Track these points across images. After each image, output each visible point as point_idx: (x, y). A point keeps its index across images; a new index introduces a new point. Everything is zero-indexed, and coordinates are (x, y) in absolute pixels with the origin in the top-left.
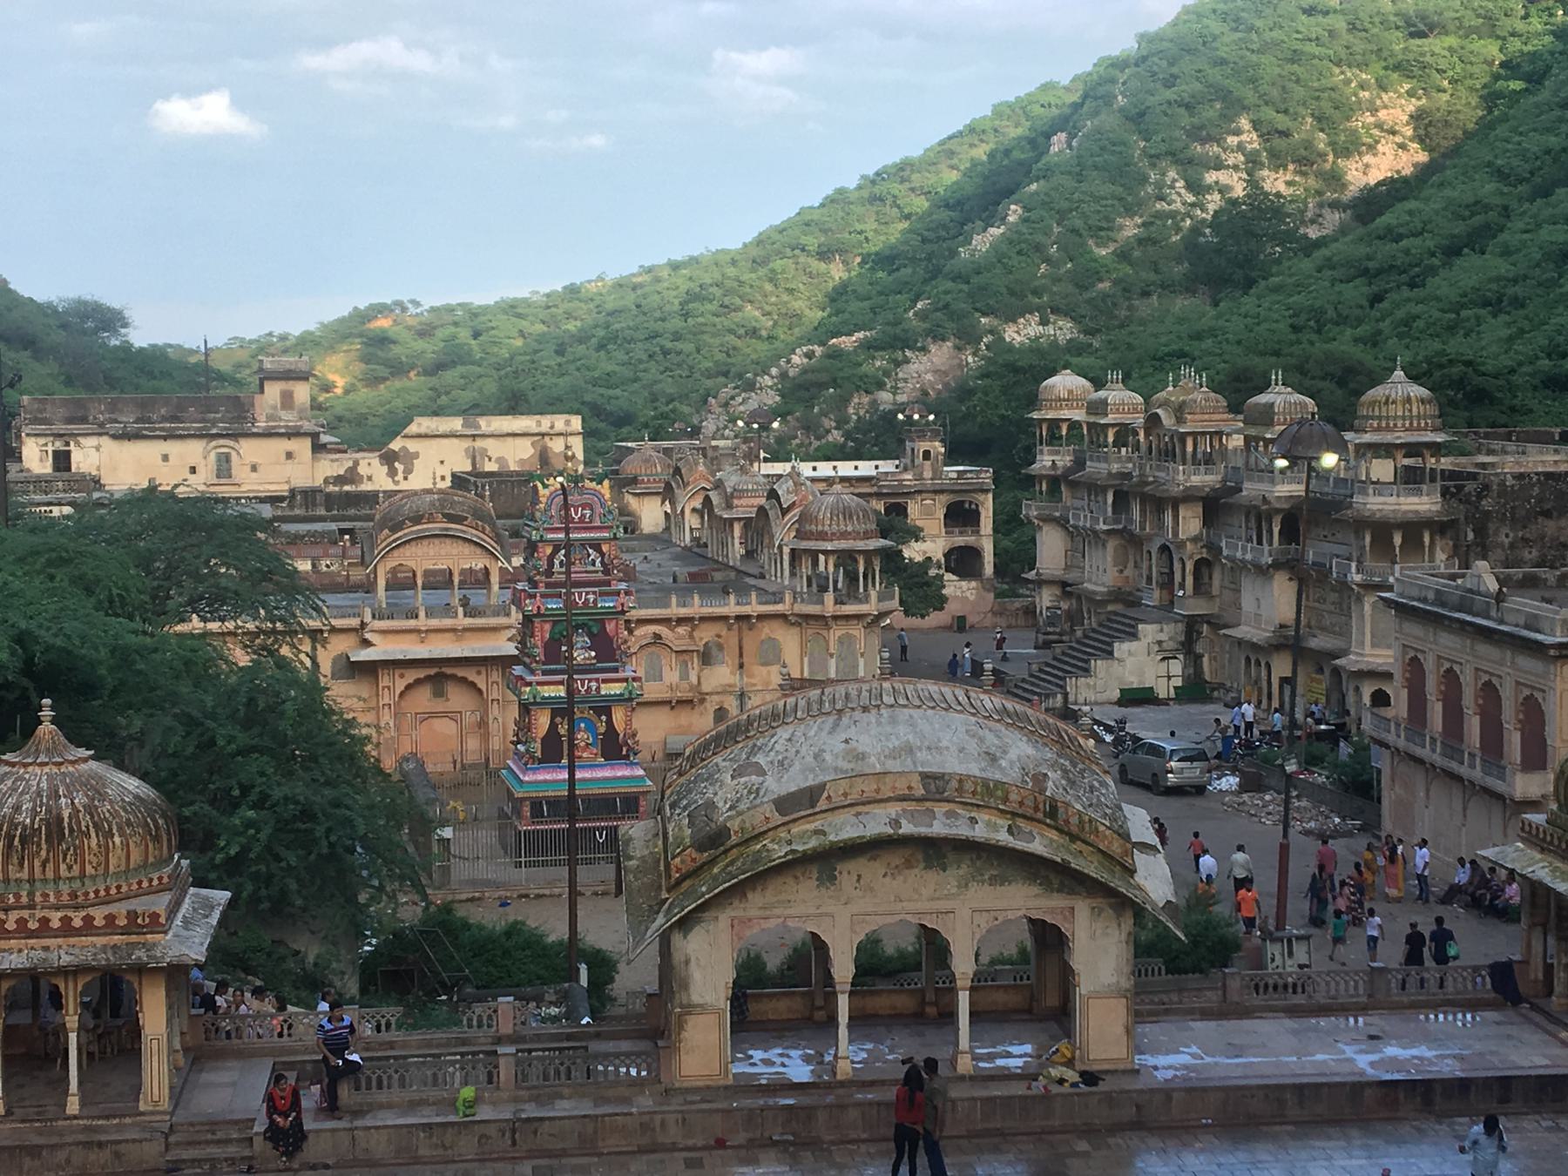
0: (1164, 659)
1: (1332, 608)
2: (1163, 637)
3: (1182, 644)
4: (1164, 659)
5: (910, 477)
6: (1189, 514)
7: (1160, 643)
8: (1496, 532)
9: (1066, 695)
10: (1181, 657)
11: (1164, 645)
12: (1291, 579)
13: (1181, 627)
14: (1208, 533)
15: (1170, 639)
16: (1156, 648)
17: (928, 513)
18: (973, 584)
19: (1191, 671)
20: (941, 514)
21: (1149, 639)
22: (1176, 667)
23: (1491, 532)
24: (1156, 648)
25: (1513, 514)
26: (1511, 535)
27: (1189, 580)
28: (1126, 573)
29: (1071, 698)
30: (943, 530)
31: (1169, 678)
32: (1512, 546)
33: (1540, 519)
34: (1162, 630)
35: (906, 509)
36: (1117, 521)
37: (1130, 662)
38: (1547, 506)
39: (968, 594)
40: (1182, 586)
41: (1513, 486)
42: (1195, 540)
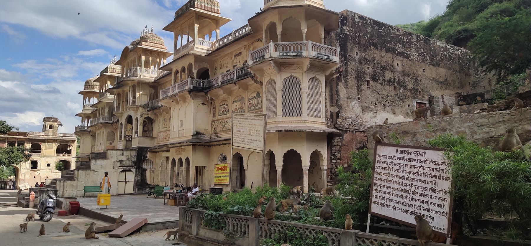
0: (123, 171)
2: (124, 158)
3: (134, 162)
4: (123, 171)
5: (43, 134)
7: (121, 161)
10: (134, 170)
11: (124, 163)
12: (203, 104)
13: (134, 153)
14: (152, 103)
15: (128, 159)
16: (119, 164)
19: (139, 178)
21: (114, 159)
22: (131, 176)
23: (349, 50)
24: (119, 164)
25: (359, 41)
26: (359, 54)
27: (140, 128)
28: (113, 144)
31: (126, 182)
32: (360, 62)
33: (372, 47)
34: (123, 155)
38: (375, 41)
40: (136, 132)
41: (359, 22)
42: (144, 107)
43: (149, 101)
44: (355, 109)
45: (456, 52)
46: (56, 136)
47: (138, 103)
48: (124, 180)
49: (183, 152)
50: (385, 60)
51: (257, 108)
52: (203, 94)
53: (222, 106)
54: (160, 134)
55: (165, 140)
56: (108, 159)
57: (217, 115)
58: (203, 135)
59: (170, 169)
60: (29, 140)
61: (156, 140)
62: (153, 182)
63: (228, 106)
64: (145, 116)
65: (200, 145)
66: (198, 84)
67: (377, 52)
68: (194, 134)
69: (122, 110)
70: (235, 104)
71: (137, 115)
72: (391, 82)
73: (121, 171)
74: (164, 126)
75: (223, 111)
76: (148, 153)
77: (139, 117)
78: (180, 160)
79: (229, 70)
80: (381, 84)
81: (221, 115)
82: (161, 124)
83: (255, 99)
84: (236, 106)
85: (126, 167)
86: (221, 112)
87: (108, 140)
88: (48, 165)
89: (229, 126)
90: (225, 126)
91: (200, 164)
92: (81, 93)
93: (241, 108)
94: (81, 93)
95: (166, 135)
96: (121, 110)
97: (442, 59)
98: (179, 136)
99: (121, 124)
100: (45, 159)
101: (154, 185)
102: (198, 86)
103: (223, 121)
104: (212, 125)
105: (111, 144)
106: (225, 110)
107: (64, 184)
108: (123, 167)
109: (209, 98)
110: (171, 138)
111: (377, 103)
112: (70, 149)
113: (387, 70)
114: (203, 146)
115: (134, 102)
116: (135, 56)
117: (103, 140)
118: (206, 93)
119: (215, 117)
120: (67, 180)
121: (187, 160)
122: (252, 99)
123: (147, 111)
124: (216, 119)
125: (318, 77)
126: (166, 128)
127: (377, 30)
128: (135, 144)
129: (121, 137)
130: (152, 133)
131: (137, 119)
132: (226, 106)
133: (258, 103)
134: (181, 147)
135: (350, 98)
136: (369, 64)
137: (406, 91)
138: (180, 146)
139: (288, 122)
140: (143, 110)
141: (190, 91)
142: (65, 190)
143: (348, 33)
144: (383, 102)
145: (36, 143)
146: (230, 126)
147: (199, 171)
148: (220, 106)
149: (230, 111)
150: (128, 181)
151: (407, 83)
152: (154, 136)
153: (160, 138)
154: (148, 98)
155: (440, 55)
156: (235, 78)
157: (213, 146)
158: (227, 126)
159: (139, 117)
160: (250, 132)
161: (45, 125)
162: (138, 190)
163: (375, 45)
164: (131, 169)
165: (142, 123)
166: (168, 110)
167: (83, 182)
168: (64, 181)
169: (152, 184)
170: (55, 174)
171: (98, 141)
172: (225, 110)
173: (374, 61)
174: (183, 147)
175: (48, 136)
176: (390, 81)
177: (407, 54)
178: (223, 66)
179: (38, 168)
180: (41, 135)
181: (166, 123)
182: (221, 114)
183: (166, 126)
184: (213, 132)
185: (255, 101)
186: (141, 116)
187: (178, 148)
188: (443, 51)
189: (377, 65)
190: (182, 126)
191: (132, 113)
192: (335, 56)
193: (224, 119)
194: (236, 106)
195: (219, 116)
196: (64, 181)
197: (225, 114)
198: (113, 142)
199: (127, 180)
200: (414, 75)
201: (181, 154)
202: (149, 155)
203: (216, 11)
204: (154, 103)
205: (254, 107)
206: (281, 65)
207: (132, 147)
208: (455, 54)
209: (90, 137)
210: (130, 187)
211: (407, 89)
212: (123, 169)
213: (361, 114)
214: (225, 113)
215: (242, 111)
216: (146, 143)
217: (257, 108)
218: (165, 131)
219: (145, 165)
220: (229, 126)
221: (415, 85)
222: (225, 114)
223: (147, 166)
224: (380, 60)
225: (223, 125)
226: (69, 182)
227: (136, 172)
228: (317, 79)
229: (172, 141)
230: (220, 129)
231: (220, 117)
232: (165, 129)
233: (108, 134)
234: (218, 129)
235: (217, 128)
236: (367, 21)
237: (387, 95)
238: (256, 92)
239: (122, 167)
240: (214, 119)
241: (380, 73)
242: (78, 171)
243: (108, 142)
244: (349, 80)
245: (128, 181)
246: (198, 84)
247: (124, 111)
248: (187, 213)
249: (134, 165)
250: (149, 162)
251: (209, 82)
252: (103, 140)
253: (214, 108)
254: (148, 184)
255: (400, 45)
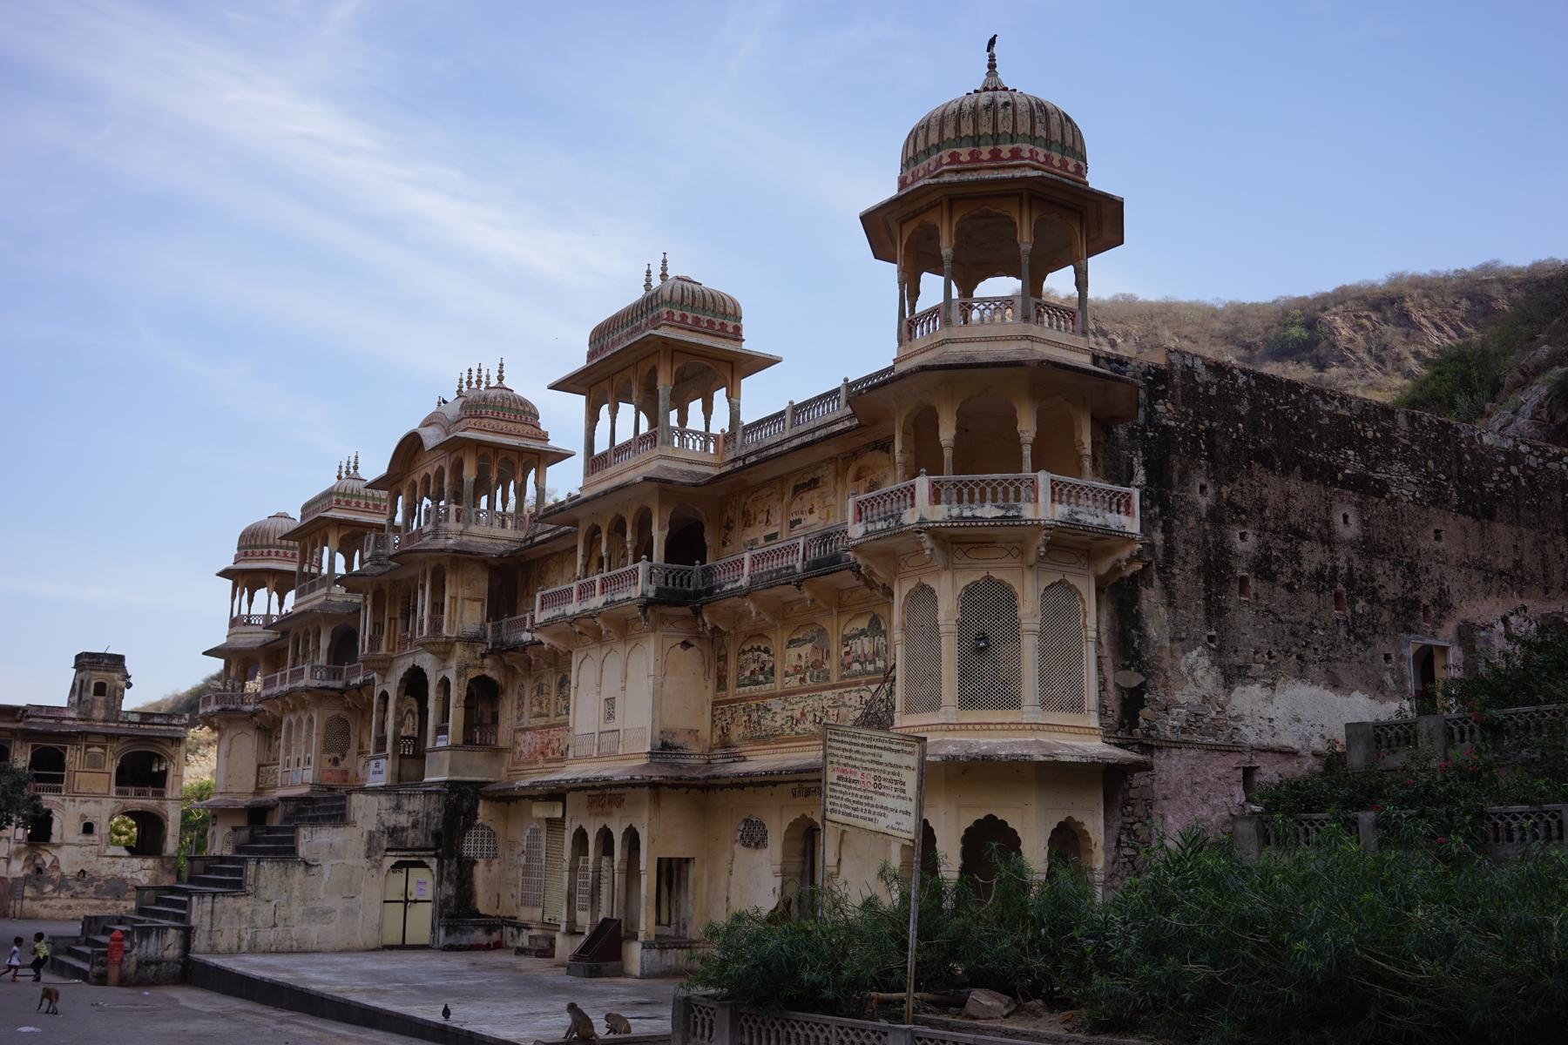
0: (398, 866)
1: (794, 682)
2: (403, 820)
4: (398, 866)
6: (463, 592)
7: (393, 832)
8: (1185, 476)
9: (187, 933)
10: (433, 863)
12: (686, 645)
13: (434, 804)
14: (497, 630)
15: (415, 825)
17: (95, 764)
18: (150, 862)
19: (449, 890)
20: (112, 767)
21: (371, 824)
22: (423, 882)
23: (1176, 480)
25: (1211, 446)
26: (1210, 490)
27: (456, 715)
28: (343, 765)
29: (200, 943)
30: (114, 788)
33: (1256, 465)
35: (62, 757)
36: (336, 675)
37: (329, 870)
39: (140, 876)
40: (442, 730)
41: (1207, 386)
42: (471, 641)
43: (488, 621)
44: (1199, 673)
45: (1551, 465)
46: (114, 721)
47: (449, 627)
48: (403, 899)
49: (614, 808)
50: (1299, 504)
51: (870, 668)
52: (686, 611)
53: (750, 655)
54: (521, 738)
55: (541, 758)
56: (353, 824)
57: (731, 681)
58: (681, 751)
59: (566, 865)
60: (28, 735)
61: (508, 757)
62: (498, 907)
63: (770, 655)
64: (473, 674)
65: (674, 787)
66: (670, 581)
67: (1272, 479)
68: (653, 746)
69: (388, 650)
70: (793, 652)
71: (444, 668)
72: (1323, 580)
73: (392, 867)
74: (536, 709)
75: (753, 673)
76: (481, 802)
77: (451, 676)
78: (606, 837)
79: (776, 534)
80: (1289, 587)
81: (745, 685)
82: (527, 701)
83: (866, 640)
84: (800, 656)
85: (408, 853)
86: (747, 673)
87: (326, 750)
88: (88, 829)
89: (773, 724)
90: (759, 724)
91: (677, 851)
92: (225, 574)
93: (817, 665)
94: (225, 574)
95: (546, 741)
96: (383, 650)
97: (1501, 491)
98: (602, 751)
99: (384, 696)
100: (77, 804)
101: (499, 917)
102: (670, 585)
103: (754, 706)
104: (713, 715)
105: (336, 762)
106: (762, 669)
107: (213, 907)
108: (399, 853)
109: (704, 625)
110: (571, 754)
111: (1274, 653)
112: (163, 768)
113: (1309, 539)
114: (685, 789)
115: (436, 625)
116: (442, 463)
117: (308, 750)
118: (697, 613)
119: (725, 689)
120: (223, 894)
121: (632, 837)
122: (855, 636)
123: (478, 655)
124: (730, 697)
125: (1071, 580)
126: (548, 716)
127: (1270, 405)
128: (437, 772)
129: (381, 742)
130: (496, 735)
131: (445, 684)
132: (764, 656)
133: (876, 653)
134: (608, 791)
135: (1182, 640)
136: (1244, 524)
137: (1376, 606)
138: (603, 793)
139: (977, 727)
140: (467, 654)
141: (647, 604)
142: (215, 929)
143: (1173, 423)
144: (1294, 649)
145: (52, 748)
146: (778, 724)
147: (672, 873)
148: (744, 652)
149: (778, 673)
150: (416, 901)
151: (1381, 580)
152: (501, 745)
153: (522, 752)
154: (482, 610)
155: (1496, 478)
156: (799, 566)
157: (718, 790)
158: (767, 722)
159: (451, 676)
160: (880, 786)
161: (78, 683)
162: (447, 934)
163: (1265, 459)
164: (426, 860)
165: (463, 698)
166: (559, 663)
167: (274, 903)
168: (214, 895)
169: (494, 915)
170: (110, 860)
171: (288, 751)
172: (762, 669)
173: (1262, 510)
174: (614, 791)
175: (88, 720)
176: (1319, 575)
177: (1376, 481)
178: (755, 519)
179: (54, 839)
180: (65, 718)
181: (545, 701)
182: (746, 681)
183: (545, 711)
184: (715, 739)
185: (864, 646)
186: (460, 674)
187: (598, 792)
188: (1507, 465)
189: (1271, 525)
190: (610, 716)
191: (427, 662)
192: (1128, 513)
193: (757, 698)
194: (800, 656)
195: (739, 686)
196: (214, 898)
197: (761, 683)
198: (344, 756)
199: (410, 898)
200: (1405, 549)
201: (609, 814)
202: (483, 811)
203: (730, 329)
204: (504, 631)
205: (861, 664)
206: (953, 543)
207: (426, 780)
208: (1550, 472)
209: (251, 732)
210: (421, 922)
211: (1379, 600)
212: (398, 859)
213: (1220, 691)
214: (761, 678)
215: (818, 677)
216: (476, 768)
217: (870, 668)
218: (544, 727)
219: (470, 847)
220: (773, 724)
221: (1409, 585)
222: (758, 683)
223: (475, 849)
224: (1283, 506)
225: (755, 717)
226: (229, 901)
227: (440, 866)
228: (1070, 587)
229: (573, 771)
230: (741, 730)
231: (744, 692)
232: (542, 721)
233: (328, 726)
234: (736, 732)
235: (733, 728)
236: (1234, 378)
237: (1311, 624)
238: (869, 617)
239: (394, 853)
240: (722, 695)
241: (1283, 551)
242: (258, 862)
243: (327, 756)
244: (1179, 578)
245: (416, 901)
246: (670, 581)
247: (393, 650)
248: (697, 1013)
249: (432, 845)
250: (483, 835)
251: (708, 573)
252: (308, 750)
253: (723, 658)
254: (477, 914)
255: (1351, 452)
